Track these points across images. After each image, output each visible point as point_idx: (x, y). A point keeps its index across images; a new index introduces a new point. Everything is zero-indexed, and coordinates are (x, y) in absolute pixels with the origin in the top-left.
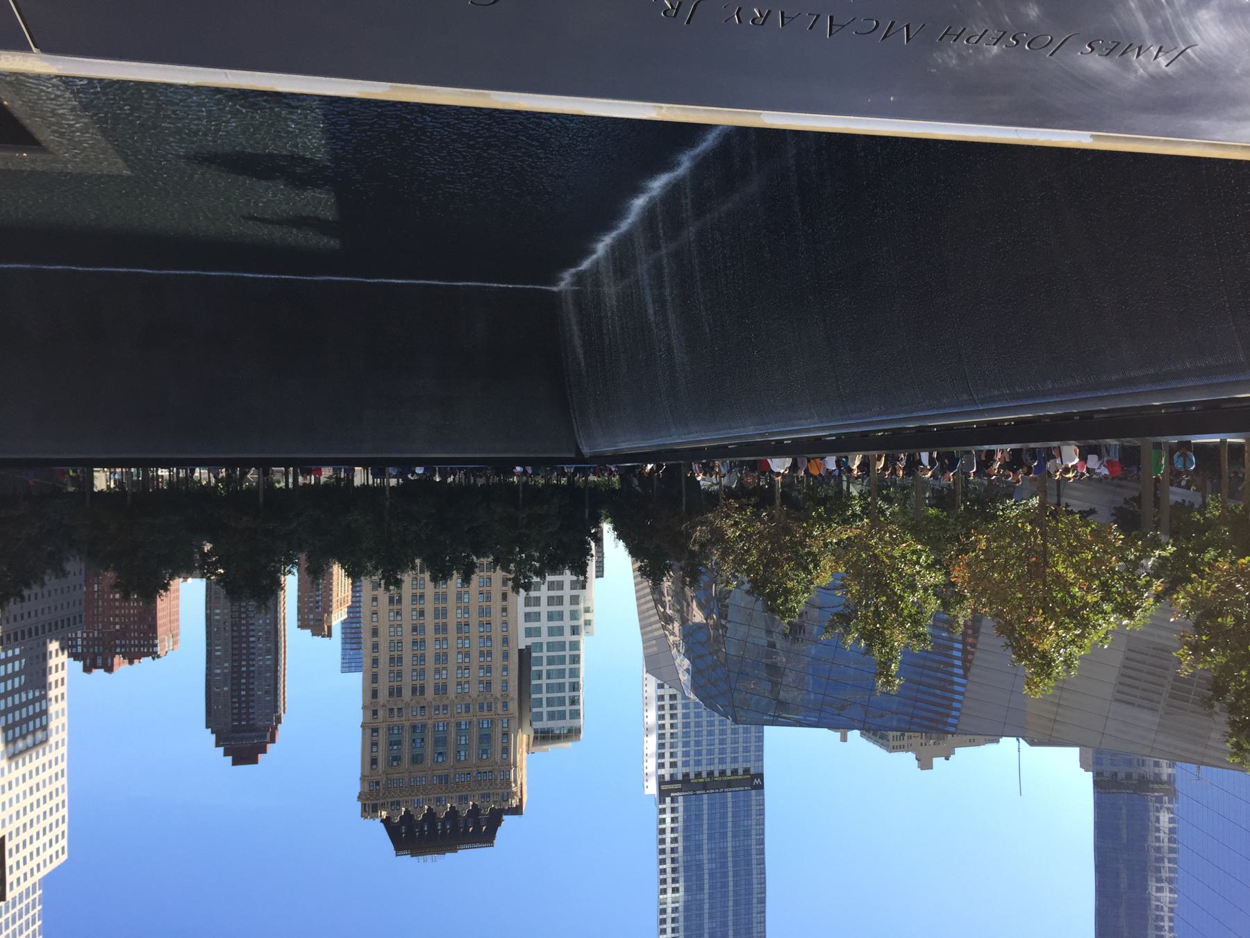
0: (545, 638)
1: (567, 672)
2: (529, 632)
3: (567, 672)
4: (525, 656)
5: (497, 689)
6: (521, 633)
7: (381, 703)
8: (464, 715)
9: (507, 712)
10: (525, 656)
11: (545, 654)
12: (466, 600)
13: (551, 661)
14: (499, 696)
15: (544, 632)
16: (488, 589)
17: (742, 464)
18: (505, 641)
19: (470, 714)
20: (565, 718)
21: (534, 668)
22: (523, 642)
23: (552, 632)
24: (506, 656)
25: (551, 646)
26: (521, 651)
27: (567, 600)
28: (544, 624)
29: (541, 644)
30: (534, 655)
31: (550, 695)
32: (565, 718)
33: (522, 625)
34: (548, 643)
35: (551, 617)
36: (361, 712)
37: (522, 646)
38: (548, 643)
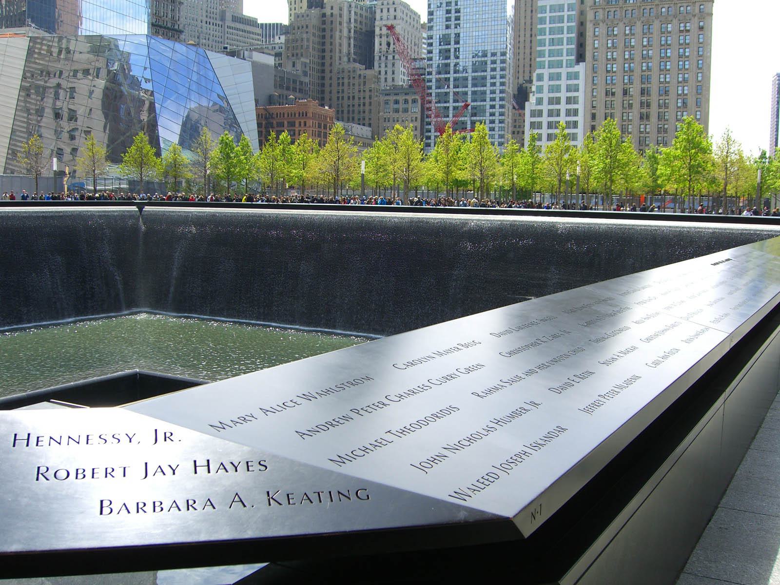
0: (564, 71)
1: (565, 42)
2: (576, 76)
3: (565, 42)
4: (580, 57)
5: (601, 30)
6: (582, 76)
7: (696, 18)
8: (629, 8)
9: (595, 10)
10: (580, 57)
11: (565, 58)
12: (679, 101)
13: (559, 53)
14: (601, 24)
15: (564, 76)
16: (660, 110)
17: (191, 200)
18: (594, 70)
19: (608, 10)
20: (551, 6)
21: (573, 46)
22: (581, 68)
23: (558, 77)
24: (594, 58)
25: (559, 64)
26: (584, 61)
27: (546, 101)
28: (563, 83)
29: (549, 68)
30: (573, 58)
31: (552, 26)
32: (551, 6)
33: (581, 82)
34: (562, 67)
35: (569, 89)
36: (714, 12)
37: (581, 63)
38: (562, 67)
